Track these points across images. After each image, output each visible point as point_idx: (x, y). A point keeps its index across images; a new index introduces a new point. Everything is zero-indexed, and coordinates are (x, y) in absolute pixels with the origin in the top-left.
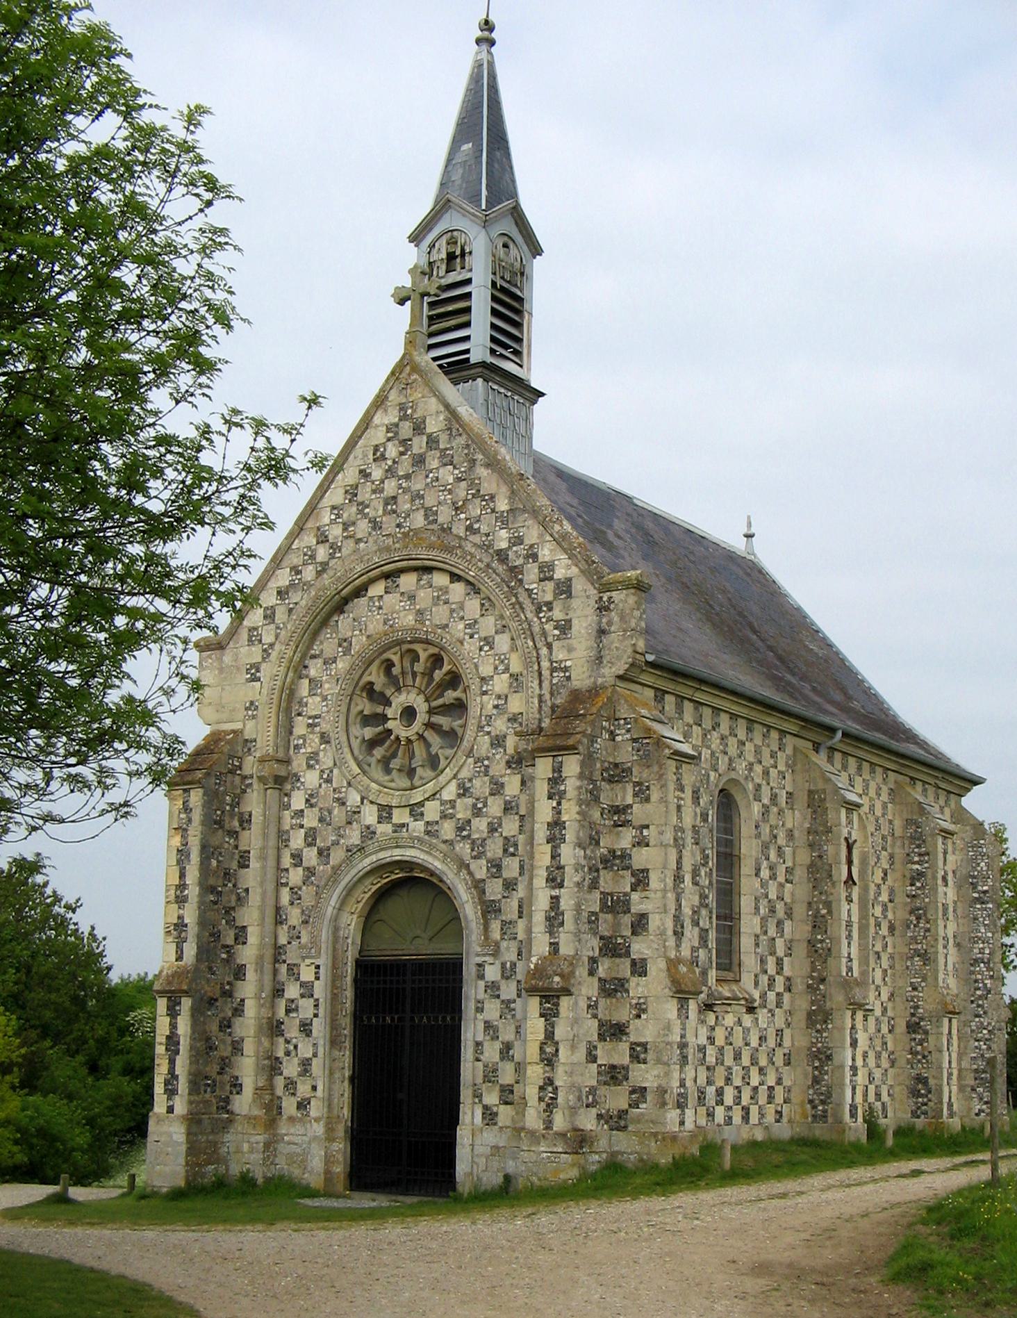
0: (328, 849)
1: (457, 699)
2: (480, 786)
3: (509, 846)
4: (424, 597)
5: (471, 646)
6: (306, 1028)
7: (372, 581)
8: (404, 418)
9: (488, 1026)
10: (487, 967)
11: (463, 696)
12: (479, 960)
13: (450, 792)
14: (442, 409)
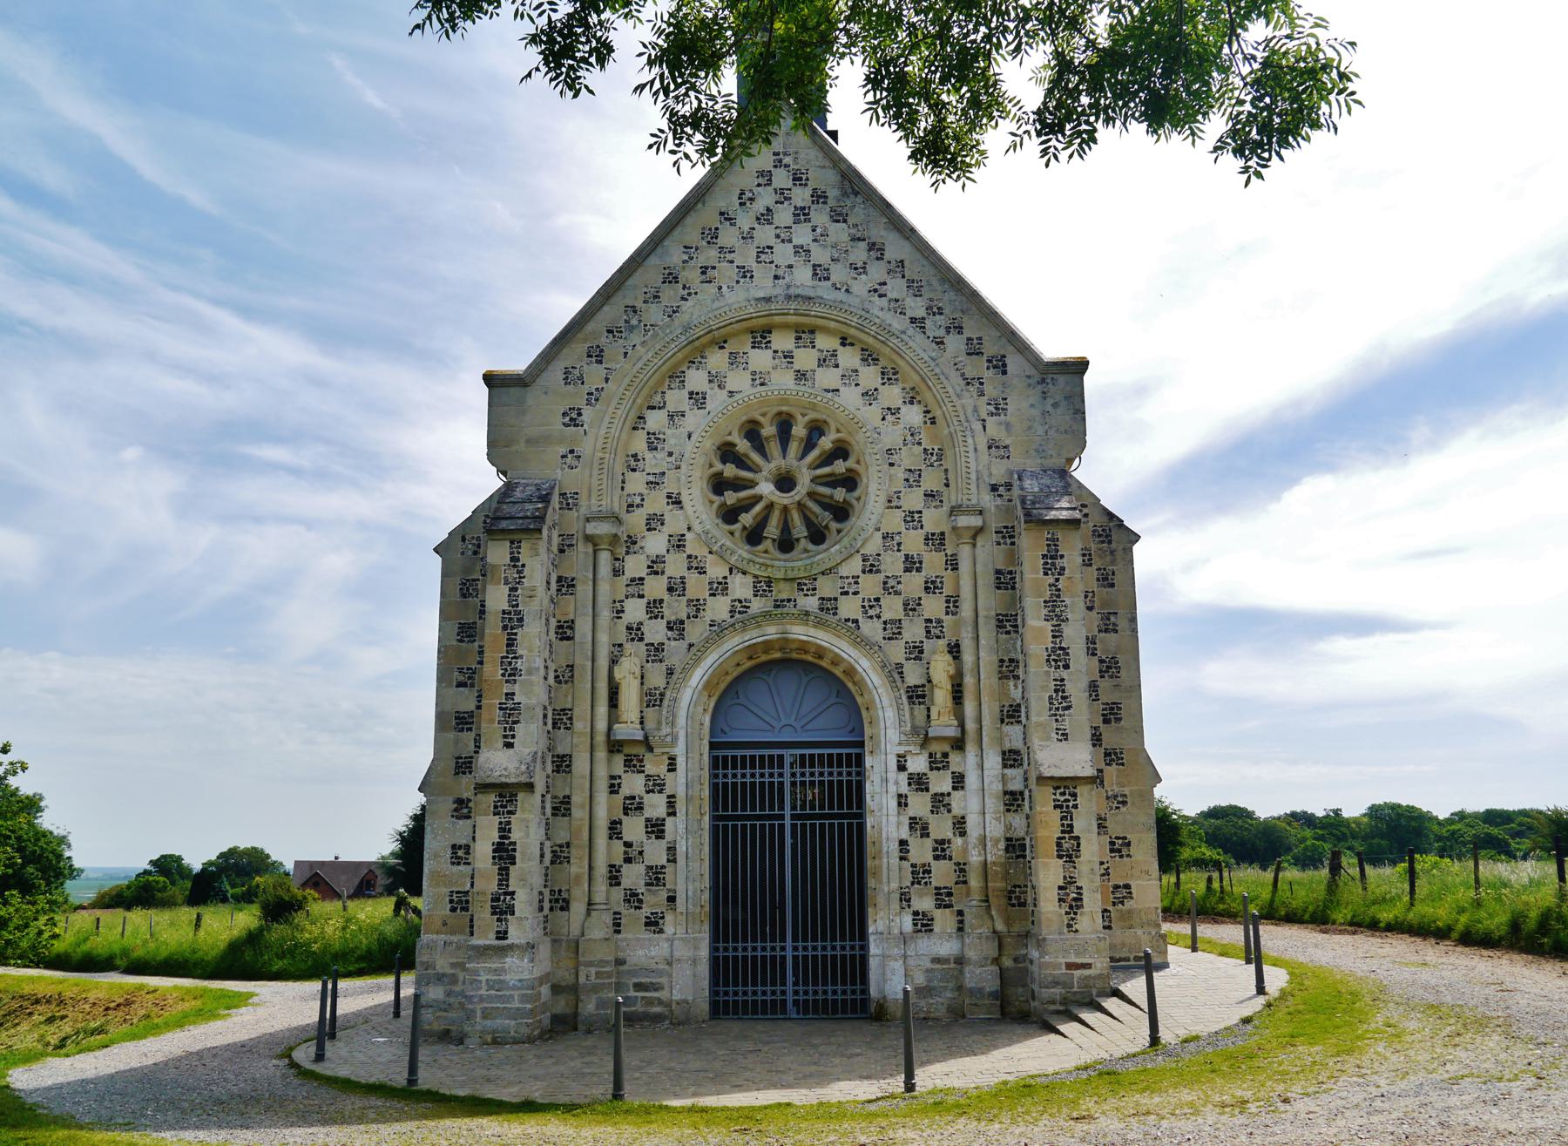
0: (682, 622)
1: (849, 470)
2: (892, 564)
3: (933, 628)
4: (806, 359)
5: (871, 414)
6: (656, 829)
7: (735, 335)
8: (778, 164)
9: (913, 822)
10: (908, 758)
11: (855, 466)
12: (902, 750)
13: (855, 566)
14: (827, 164)
